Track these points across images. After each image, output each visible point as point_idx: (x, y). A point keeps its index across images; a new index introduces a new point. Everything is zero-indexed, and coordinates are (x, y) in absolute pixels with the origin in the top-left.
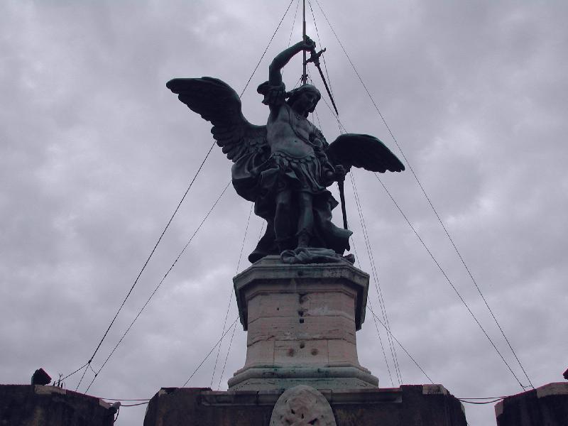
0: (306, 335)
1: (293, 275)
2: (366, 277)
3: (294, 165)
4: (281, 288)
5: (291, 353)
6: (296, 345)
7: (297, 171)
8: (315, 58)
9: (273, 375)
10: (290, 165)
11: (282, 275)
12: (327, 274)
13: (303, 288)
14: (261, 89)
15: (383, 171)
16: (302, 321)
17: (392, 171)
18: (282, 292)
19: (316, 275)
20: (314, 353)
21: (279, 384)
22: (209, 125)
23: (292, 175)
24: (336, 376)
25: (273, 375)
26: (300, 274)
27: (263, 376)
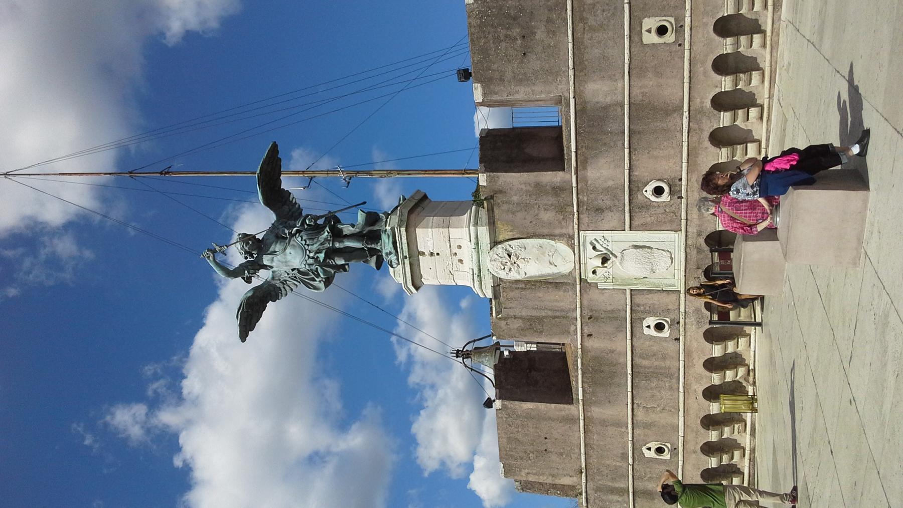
1: (407, 261)
6: (456, 259)
7: (319, 251)
9: (479, 276)
10: (313, 258)
12: (404, 241)
16: (438, 254)
19: (405, 247)
20: (460, 247)
21: (484, 272)
23: (322, 256)
24: (477, 238)
25: (479, 276)
26: (406, 257)
27: (480, 281)
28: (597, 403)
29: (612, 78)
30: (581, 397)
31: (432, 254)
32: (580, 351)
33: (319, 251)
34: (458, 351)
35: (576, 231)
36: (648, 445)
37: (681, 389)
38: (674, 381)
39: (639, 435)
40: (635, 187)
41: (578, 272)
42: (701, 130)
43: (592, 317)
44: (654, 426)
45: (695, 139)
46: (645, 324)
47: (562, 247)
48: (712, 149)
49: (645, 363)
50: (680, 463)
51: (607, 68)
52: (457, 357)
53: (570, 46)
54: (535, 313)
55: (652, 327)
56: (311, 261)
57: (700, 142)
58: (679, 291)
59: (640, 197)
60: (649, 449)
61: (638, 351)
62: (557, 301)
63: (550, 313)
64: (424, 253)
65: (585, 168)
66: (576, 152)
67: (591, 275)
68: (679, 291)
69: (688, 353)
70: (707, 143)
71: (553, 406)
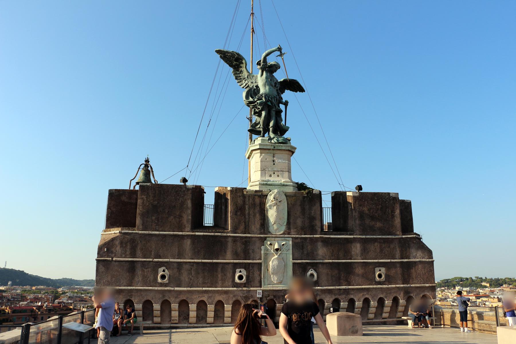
0: (275, 169)
1: (272, 148)
2: (296, 148)
3: (270, 99)
4: (267, 151)
5: (270, 176)
6: (272, 173)
7: (272, 103)
8: (281, 55)
11: (268, 147)
12: (284, 148)
13: (275, 152)
14: (259, 64)
15: (297, 92)
17: (300, 92)
18: (267, 153)
19: (280, 148)
20: (278, 176)
22: (232, 70)
23: (269, 103)
24: (287, 186)
25: (266, 184)
26: (274, 147)
28: (193, 243)
29: (362, 254)
30: (197, 233)
31: (274, 161)
32: (225, 234)
33: (272, 103)
34: (149, 162)
35: (292, 236)
36: (166, 271)
37: (204, 289)
38: (209, 285)
39: (173, 265)
40: (314, 266)
41: (271, 236)
42: (340, 295)
43: (246, 242)
44: (179, 274)
45: (336, 292)
46: (242, 270)
47: (283, 228)
48: (331, 300)
49: (219, 269)
50: (156, 288)
51: (365, 253)
52: (146, 161)
53: (375, 237)
54: (247, 212)
55: (240, 273)
56: (267, 98)
57: (335, 295)
58: (261, 287)
59: (309, 267)
60: (164, 271)
61: (227, 266)
62: (254, 224)
63: (247, 220)
64: (274, 157)
65: (322, 241)
66: (330, 238)
67: (269, 243)
68: (261, 287)
69: (226, 292)
70: (334, 298)
71: (190, 217)
